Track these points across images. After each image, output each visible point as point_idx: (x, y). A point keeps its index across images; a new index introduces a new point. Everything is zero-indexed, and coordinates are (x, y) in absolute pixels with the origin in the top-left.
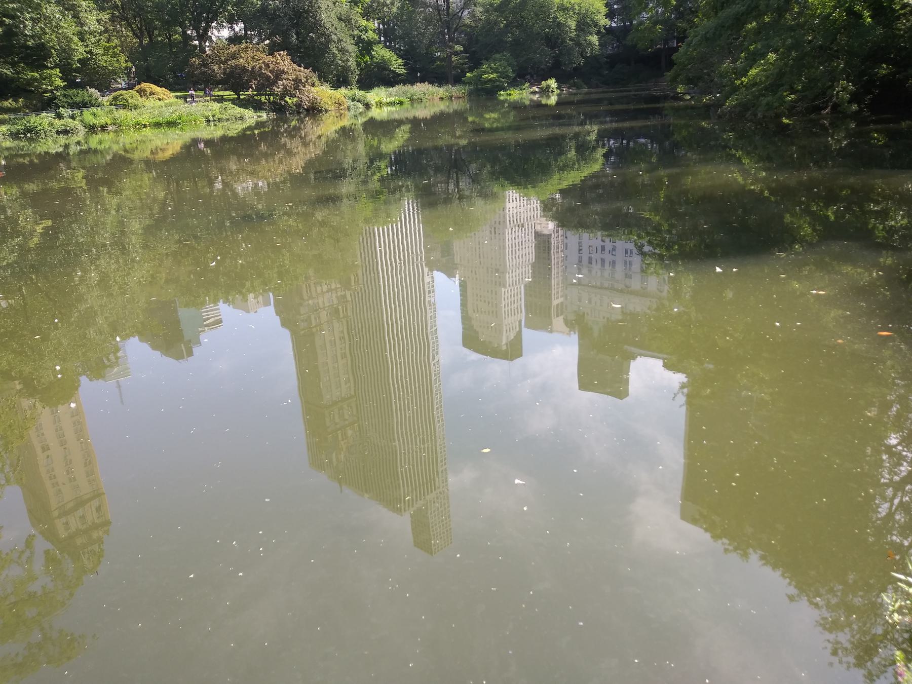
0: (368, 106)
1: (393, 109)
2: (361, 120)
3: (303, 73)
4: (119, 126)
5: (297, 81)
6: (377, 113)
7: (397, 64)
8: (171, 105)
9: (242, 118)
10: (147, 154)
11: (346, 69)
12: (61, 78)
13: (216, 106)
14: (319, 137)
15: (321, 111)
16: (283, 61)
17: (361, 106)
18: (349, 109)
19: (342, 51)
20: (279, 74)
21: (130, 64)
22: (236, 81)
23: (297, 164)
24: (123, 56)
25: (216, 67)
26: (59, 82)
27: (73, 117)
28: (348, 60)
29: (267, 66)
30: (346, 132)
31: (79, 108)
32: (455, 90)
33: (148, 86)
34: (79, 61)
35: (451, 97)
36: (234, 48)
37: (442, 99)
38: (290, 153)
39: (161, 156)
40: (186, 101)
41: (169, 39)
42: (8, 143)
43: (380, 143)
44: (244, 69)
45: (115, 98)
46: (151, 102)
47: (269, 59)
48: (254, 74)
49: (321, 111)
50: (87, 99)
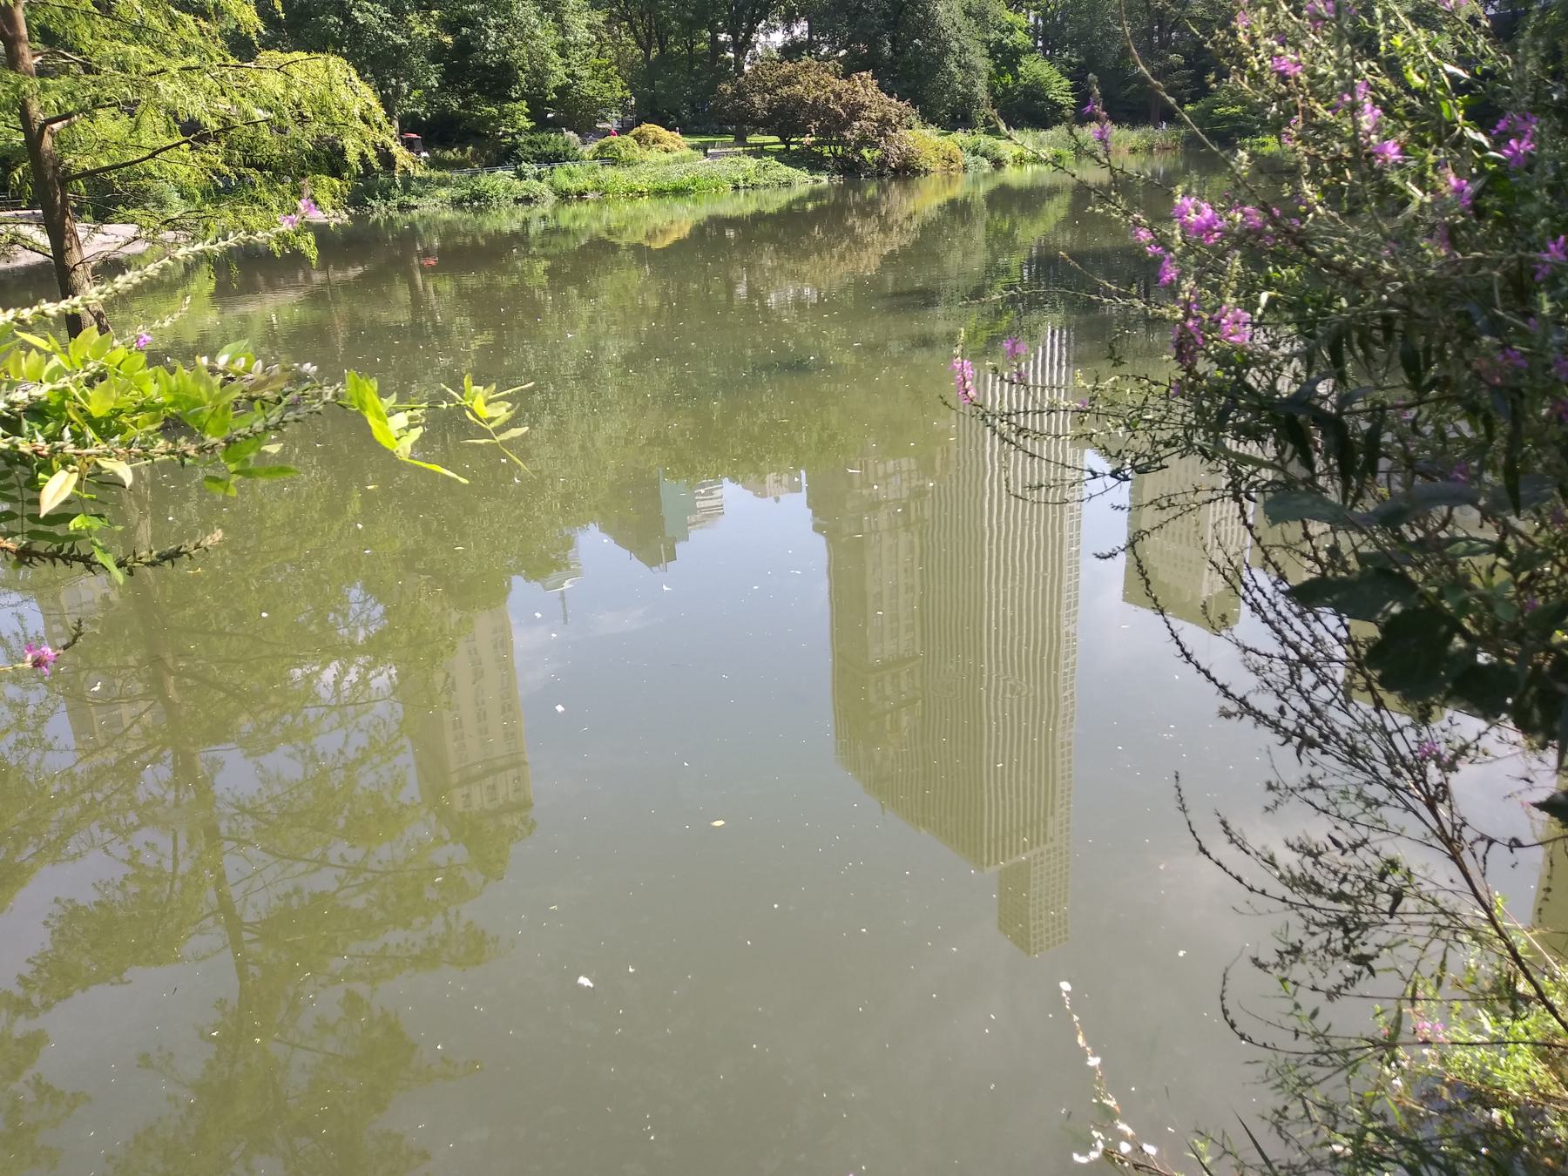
0: (998, 164)
1: (1043, 168)
2: (983, 189)
3: (896, 107)
4: (603, 192)
5: (884, 122)
6: (1013, 176)
7: (1059, 89)
8: (683, 160)
9: (788, 184)
10: (640, 238)
11: (969, 99)
12: (527, 115)
13: (750, 163)
14: (910, 218)
15: (917, 172)
16: (865, 88)
17: (986, 162)
18: (965, 168)
19: (966, 67)
20: (855, 111)
21: (628, 93)
22: (786, 119)
23: (868, 263)
24: (619, 80)
25: (757, 99)
26: (525, 123)
27: (539, 178)
28: (973, 84)
29: (838, 96)
30: (958, 210)
31: (549, 162)
32: (1162, 134)
33: (651, 129)
34: (556, 90)
35: (1151, 147)
36: (788, 67)
37: (1133, 151)
38: (858, 243)
39: (658, 244)
40: (706, 155)
41: (690, 49)
42: (448, 215)
43: (1013, 225)
44: (800, 102)
45: (602, 148)
46: (654, 155)
47: (844, 84)
48: (817, 110)
49: (917, 172)
50: (561, 148)
